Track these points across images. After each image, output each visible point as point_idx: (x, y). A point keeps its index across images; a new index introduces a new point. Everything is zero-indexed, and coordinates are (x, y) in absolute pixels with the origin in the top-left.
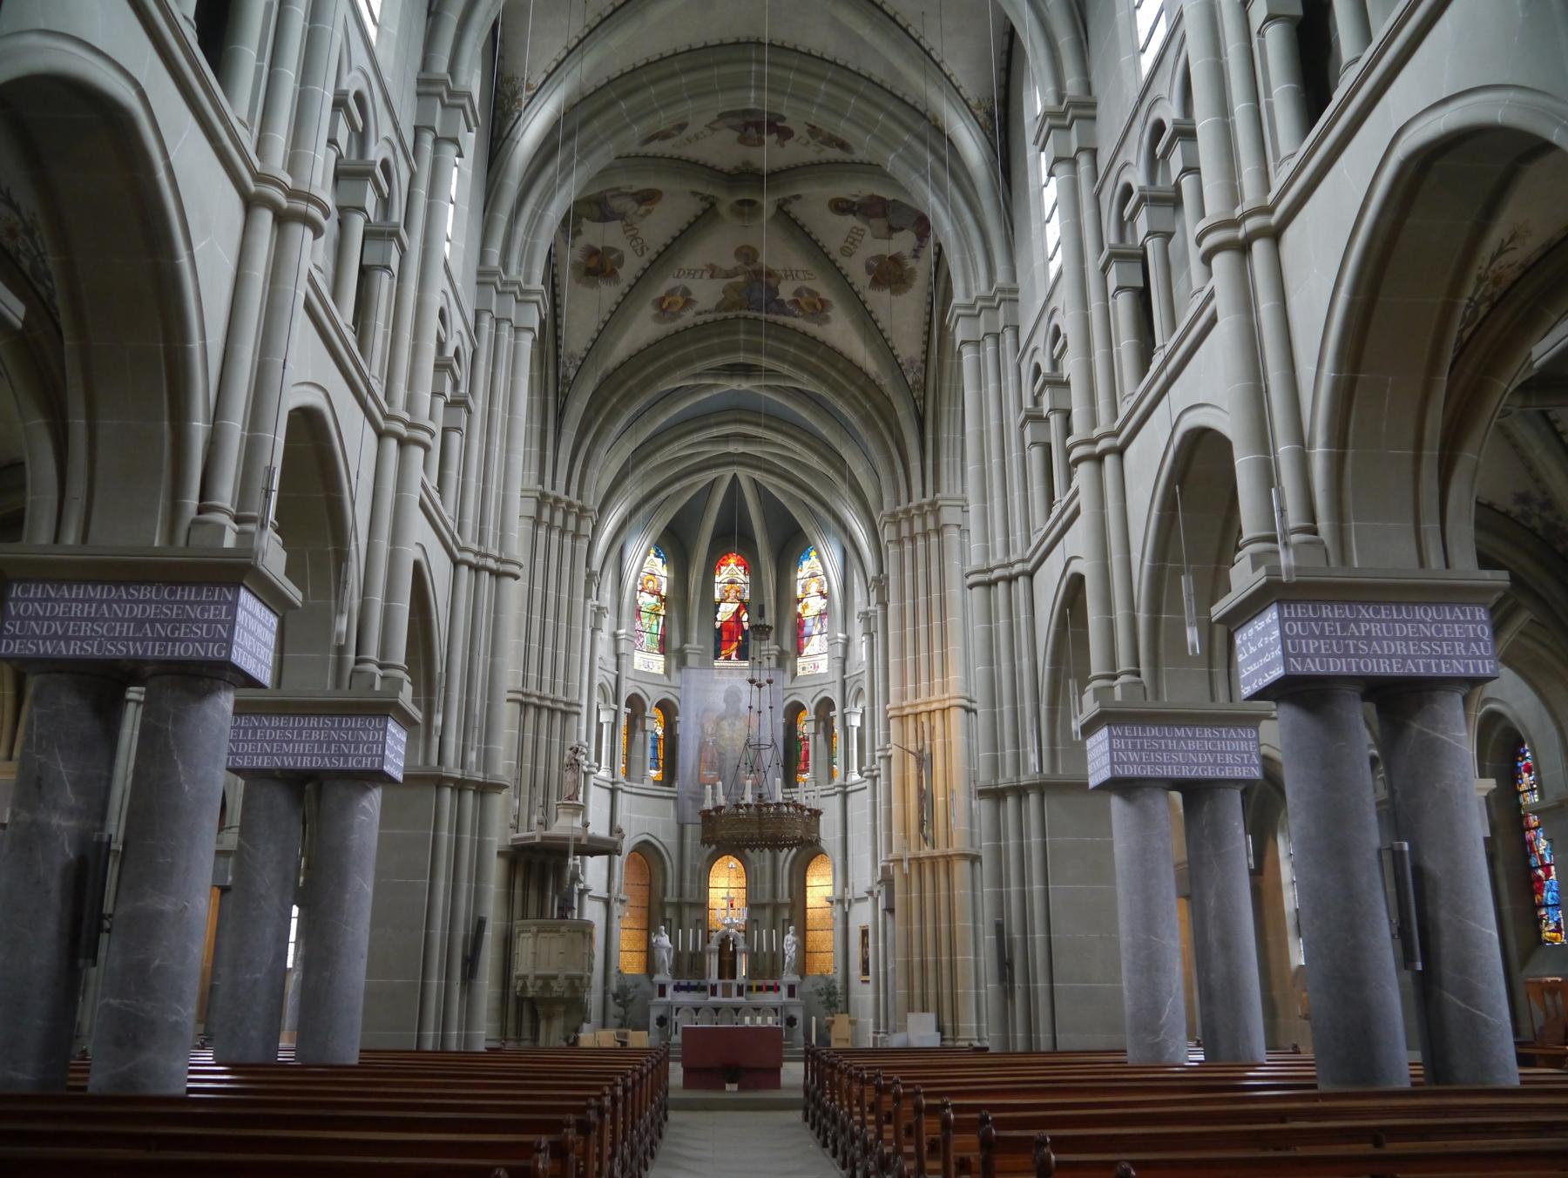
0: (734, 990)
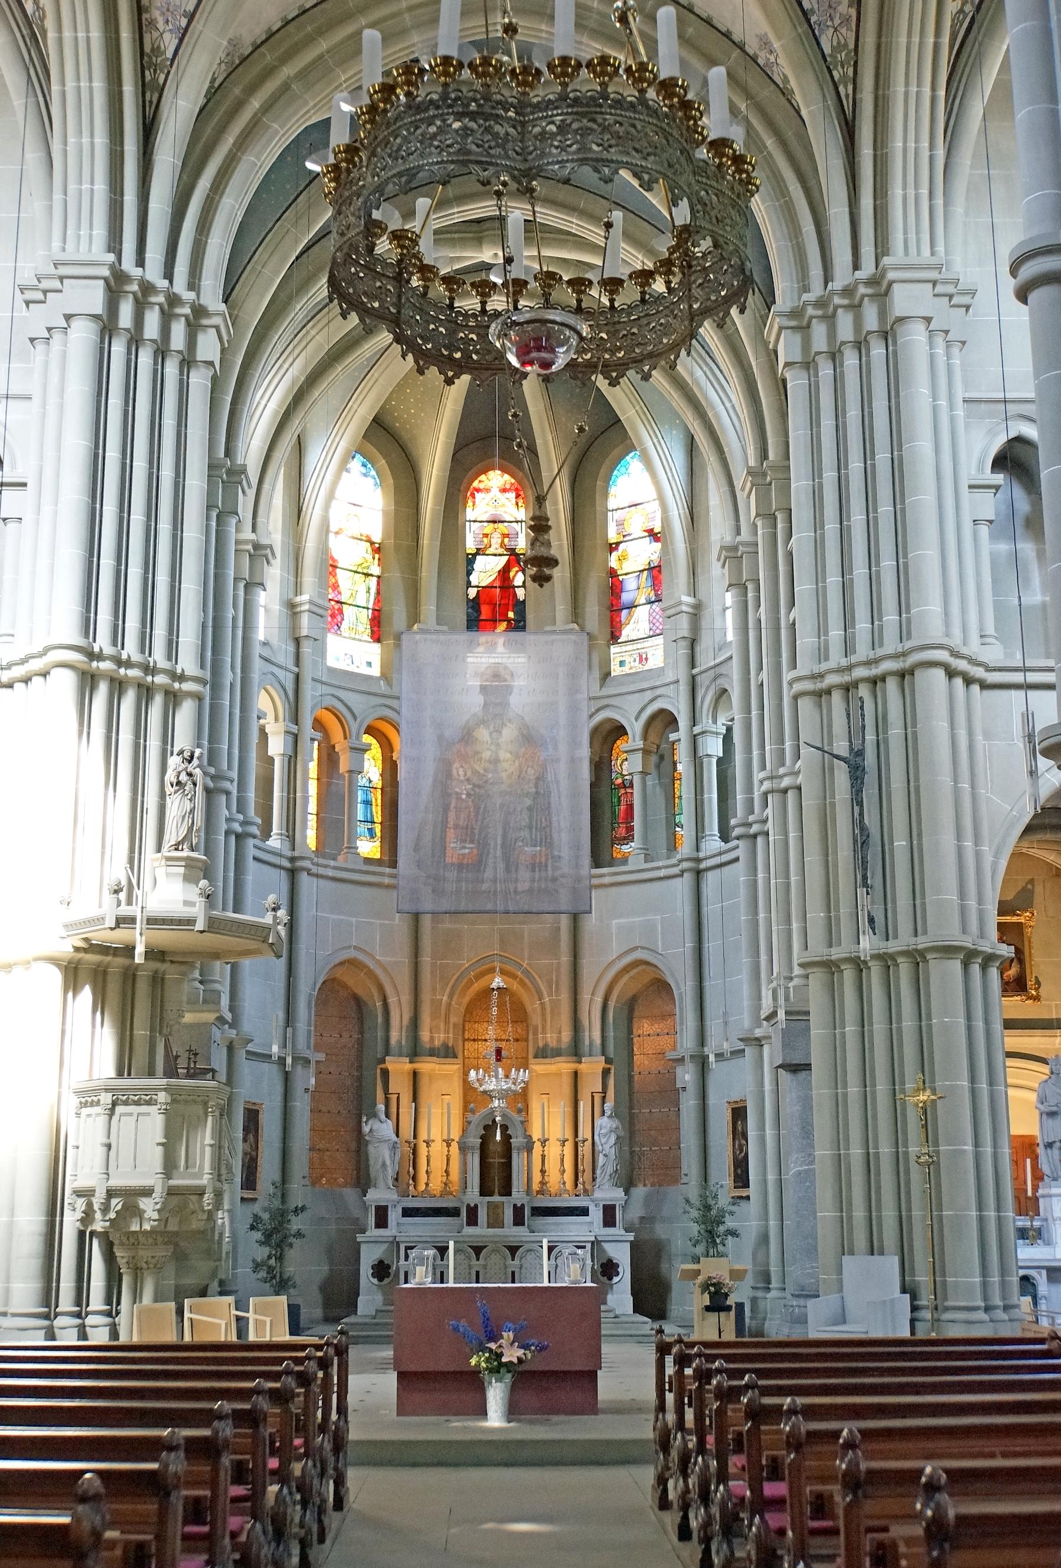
0: (509, 1215)
